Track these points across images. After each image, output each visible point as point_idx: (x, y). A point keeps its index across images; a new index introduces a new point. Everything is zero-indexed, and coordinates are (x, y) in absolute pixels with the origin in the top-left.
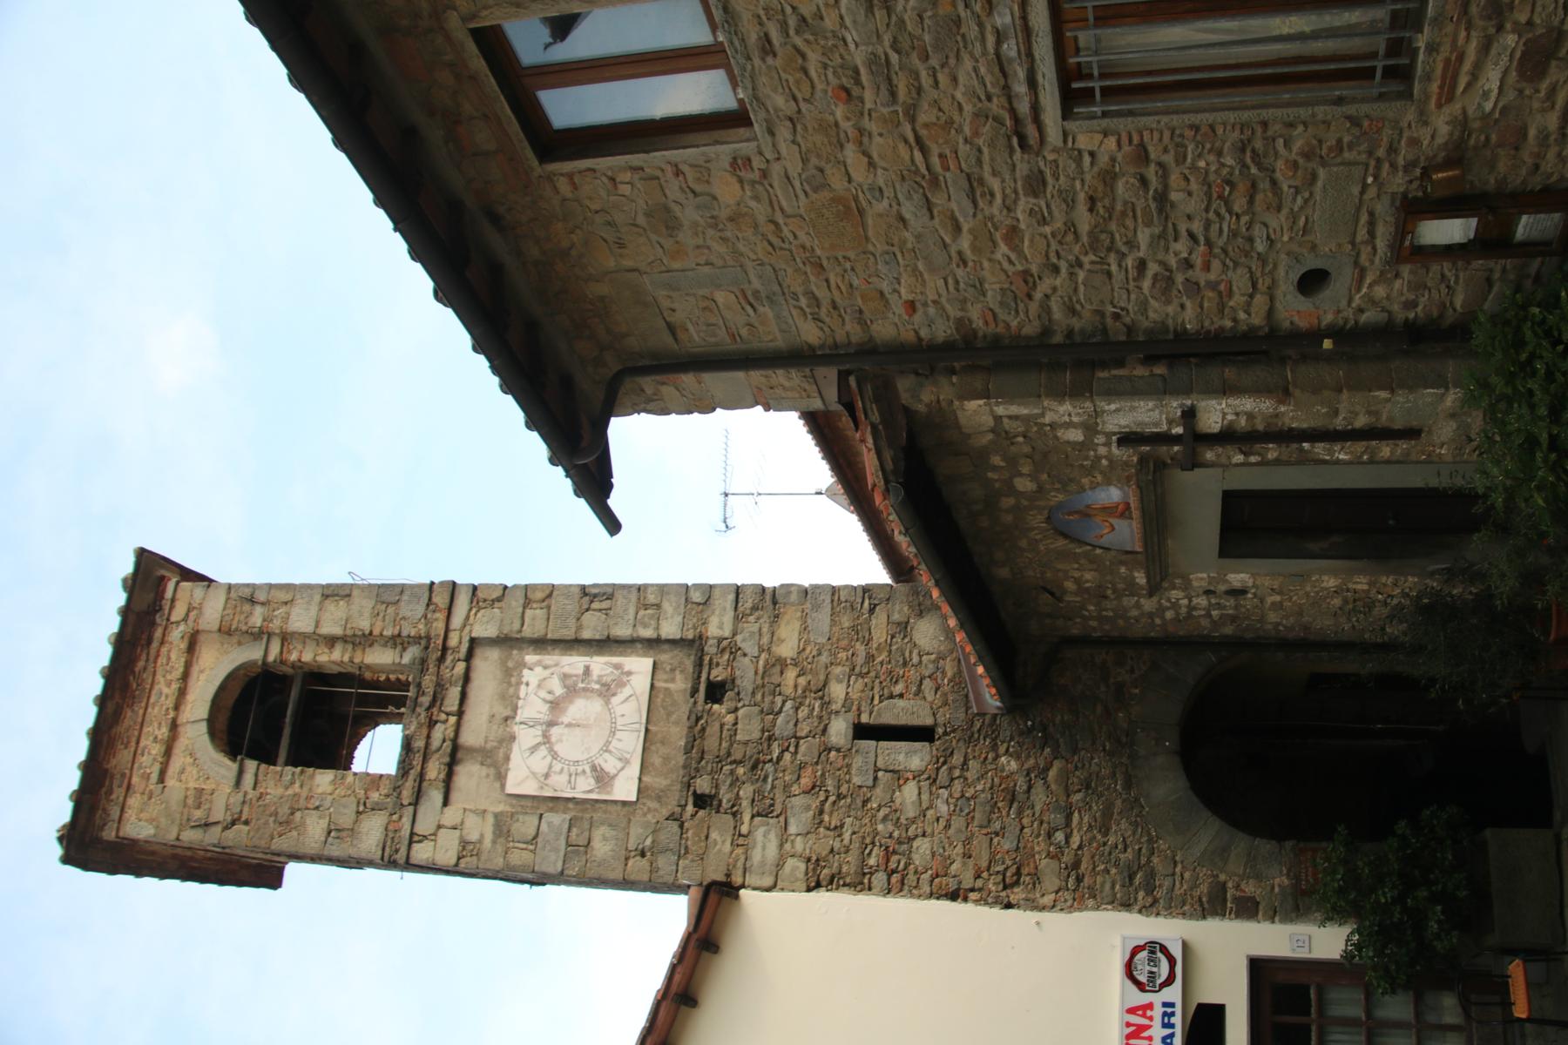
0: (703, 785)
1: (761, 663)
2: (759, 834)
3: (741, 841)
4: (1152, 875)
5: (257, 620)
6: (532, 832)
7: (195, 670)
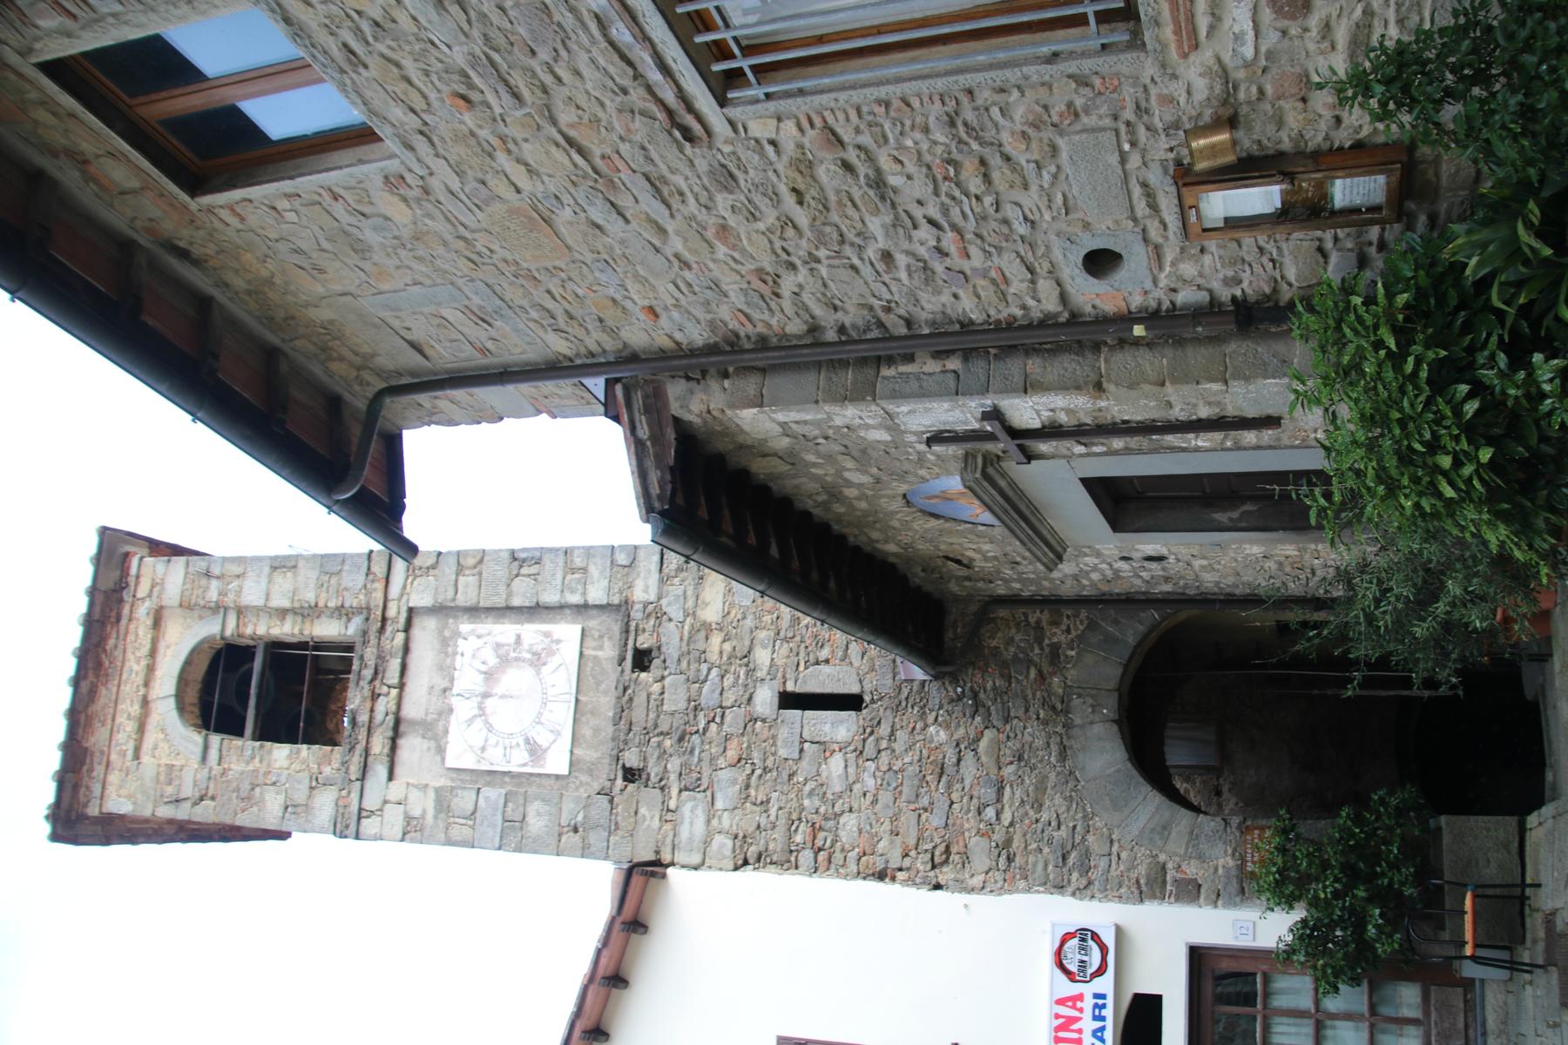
0: (631, 759)
1: (686, 628)
2: (686, 809)
3: (669, 817)
4: (1087, 854)
5: (213, 595)
6: (471, 808)
7: (162, 645)
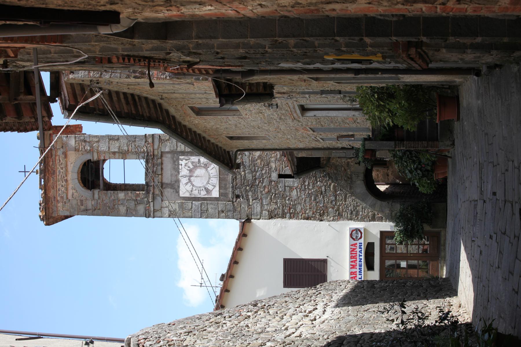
0: (237, 192)
2: (255, 205)
6: (190, 207)
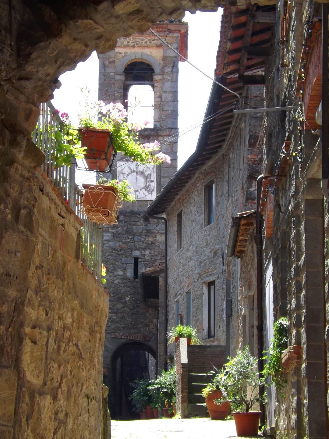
2: (109, 234)
